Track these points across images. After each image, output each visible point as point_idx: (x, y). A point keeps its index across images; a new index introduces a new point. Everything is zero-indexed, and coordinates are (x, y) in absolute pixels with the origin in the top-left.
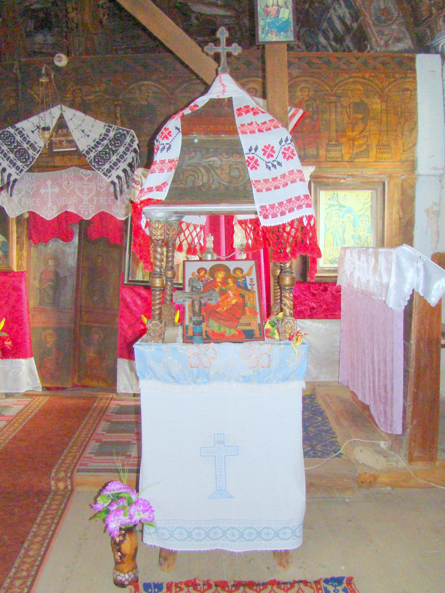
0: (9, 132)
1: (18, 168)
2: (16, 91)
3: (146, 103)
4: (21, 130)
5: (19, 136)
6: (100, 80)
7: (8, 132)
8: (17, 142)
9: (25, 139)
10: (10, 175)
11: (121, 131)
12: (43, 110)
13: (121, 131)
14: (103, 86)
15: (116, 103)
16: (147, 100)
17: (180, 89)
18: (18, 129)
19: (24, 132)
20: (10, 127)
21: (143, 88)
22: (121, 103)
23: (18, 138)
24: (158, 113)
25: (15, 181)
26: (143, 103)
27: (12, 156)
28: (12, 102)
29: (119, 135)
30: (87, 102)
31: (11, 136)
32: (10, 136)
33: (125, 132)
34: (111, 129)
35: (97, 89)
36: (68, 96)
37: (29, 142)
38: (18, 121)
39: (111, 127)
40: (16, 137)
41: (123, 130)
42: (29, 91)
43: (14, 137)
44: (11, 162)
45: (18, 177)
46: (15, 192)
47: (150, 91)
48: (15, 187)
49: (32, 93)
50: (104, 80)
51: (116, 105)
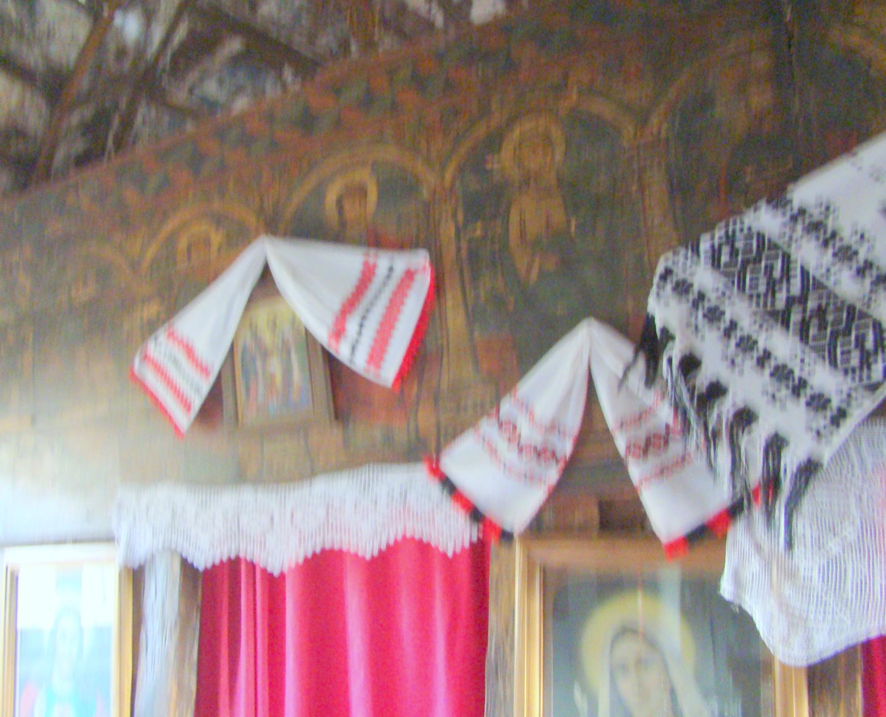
1: (818, 402)
8: (805, 273)
9: (846, 254)
10: (775, 445)
20: (763, 206)
23: (808, 254)
25: (809, 469)
27: (783, 345)
37: (868, 265)
38: (799, 172)
44: (782, 373)
45: (826, 454)
46: (801, 525)
48: (806, 504)
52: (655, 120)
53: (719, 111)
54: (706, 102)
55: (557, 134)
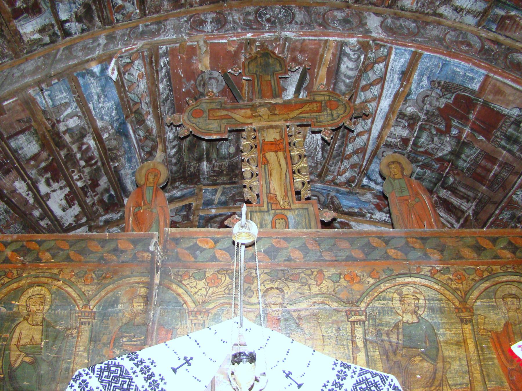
0: (122, 367)
2: (149, 286)
3: (415, 320)
4: (148, 363)
5: (141, 377)
6: (321, 272)
7: (119, 366)
11: (368, 376)
12: (197, 326)
13: (368, 376)
14: (327, 285)
15: (354, 318)
16: (415, 312)
17: (476, 293)
18: (142, 361)
19: (153, 369)
21: (405, 290)
22: (363, 317)
24: (441, 339)
26: (409, 318)
28: (138, 307)
29: (364, 386)
30: (295, 314)
31: (125, 375)
32: (121, 376)
33: (377, 379)
34: (349, 373)
35: (315, 289)
36: (254, 300)
39: (349, 367)
40: (135, 379)
41: (374, 375)
42: (174, 286)
43: (130, 379)
47: (421, 297)
49: (180, 291)
50: (327, 274)
51: (353, 323)
52: (92, 303)
53: (120, 307)
54: (115, 302)
55: (48, 296)
